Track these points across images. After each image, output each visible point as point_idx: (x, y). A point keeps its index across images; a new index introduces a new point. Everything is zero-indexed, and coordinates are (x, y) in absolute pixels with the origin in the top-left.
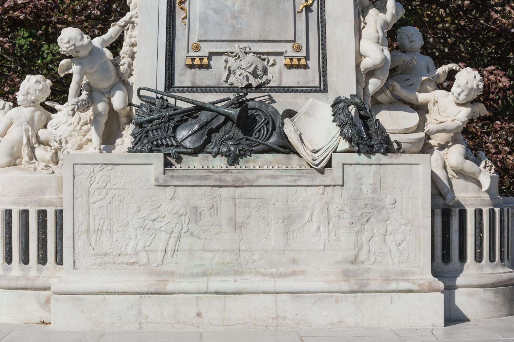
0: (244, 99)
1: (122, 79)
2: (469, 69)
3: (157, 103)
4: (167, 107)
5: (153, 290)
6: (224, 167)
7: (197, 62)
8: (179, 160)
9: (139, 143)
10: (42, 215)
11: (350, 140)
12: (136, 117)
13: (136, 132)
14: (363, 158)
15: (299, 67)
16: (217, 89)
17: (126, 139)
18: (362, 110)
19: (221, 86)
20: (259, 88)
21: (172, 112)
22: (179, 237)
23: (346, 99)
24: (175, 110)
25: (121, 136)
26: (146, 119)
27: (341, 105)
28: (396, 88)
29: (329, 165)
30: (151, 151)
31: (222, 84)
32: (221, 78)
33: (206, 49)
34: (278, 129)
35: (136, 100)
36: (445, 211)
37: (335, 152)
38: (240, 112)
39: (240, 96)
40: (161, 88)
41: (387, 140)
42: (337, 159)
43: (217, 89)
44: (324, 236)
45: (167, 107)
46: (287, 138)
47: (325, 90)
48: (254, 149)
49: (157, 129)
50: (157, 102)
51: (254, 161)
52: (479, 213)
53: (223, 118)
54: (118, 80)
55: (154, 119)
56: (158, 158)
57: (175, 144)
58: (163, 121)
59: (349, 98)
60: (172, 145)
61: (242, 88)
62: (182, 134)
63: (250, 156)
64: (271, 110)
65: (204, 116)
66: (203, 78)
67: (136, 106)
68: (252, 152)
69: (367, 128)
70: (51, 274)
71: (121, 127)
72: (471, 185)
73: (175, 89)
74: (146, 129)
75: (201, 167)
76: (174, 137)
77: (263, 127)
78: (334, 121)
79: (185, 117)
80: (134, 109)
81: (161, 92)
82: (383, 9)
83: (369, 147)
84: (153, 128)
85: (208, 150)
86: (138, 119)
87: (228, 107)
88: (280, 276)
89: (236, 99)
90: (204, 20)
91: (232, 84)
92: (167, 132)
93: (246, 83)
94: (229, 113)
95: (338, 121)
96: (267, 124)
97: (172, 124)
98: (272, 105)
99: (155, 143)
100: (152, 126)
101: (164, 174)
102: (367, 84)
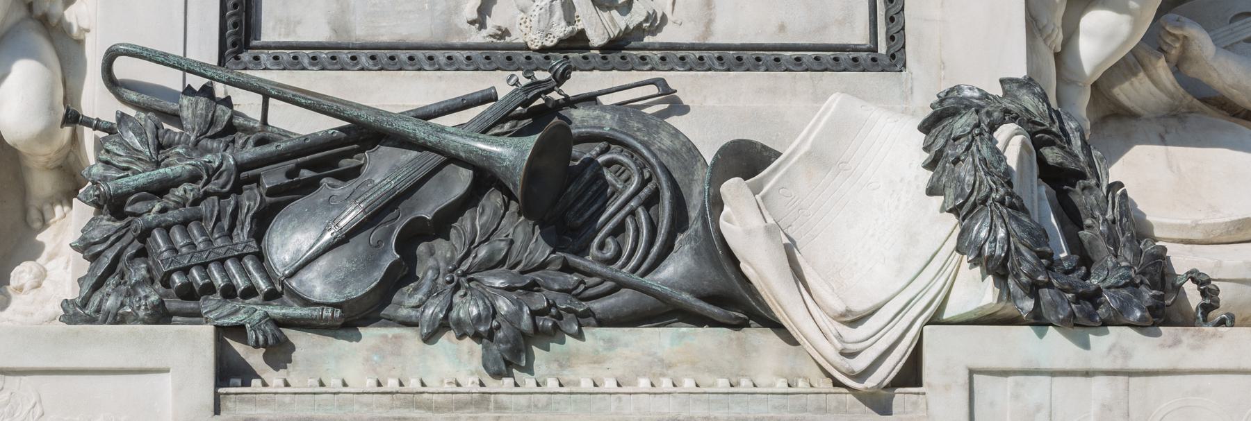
0: (554, 95)
1: (38, 12)
3: (186, 114)
4: (230, 129)
6: (469, 384)
8: (279, 354)
9: (112, 281)
11: (999, 270)
12: (98, 170)
13: (96, 235)
14: (1055, 346)
16: (441, 56)
18: (1050, 143)
19: (456, 41)
20: (618, 49)
21: (250, 153)
23: (985, 96)
24: (261, 142)
25: (34, 251)
26: (141, 179)
27: (962, 124)
28: (1195, 49)
29: (911, 374)
30: (160, 315)
31: (460, 32)
32: (457, 9)
34: (695, 225)
35: (96, 101)
37: (935, 320)
38: (538, 151)
39: (536, 84)
40: (205, 49)
41: (1157, 270)
42: (947, 353)
43: (441, 56)
45: (230, 129)
46: (735, 262)
47: (895, 61)
48: (596, 306)
49: (185, 224)
50: (189, 109)
51: (597, 360)
53: (462, 179)
54: (21, 13)
55: (175, 182)
56: (191, 346)
57: (263, 285)
58: (211, 187)
59: (997, 91)
60: (250, 292)
61: (543, 49)
62: (291, 242)
63: (579, 336)
64: (666, 141)
67: (96, 125)
68: (588, 318)
69: (1071, 217)
71: (34, 214)
73: (264, 56)
74: (140, 222)
75: (370, 384)
76: (260, 257)
77: (633, 213)
78: (931, 191)
79: (306, 174)
80: (89, 136)
81: (202, 64)
83: (1079, 298)
84: (170, 216)
85: (403, 312)
86: (105, 179)
87: (485, 129)
89: (522, 97)
91: (505, 33)
92: (229, 234)
93: (560, 30)
94: (489, 156)
95: (950, 192)
96: (652, 200)
97: (251, 201)
98: (674, 121)
99: (177, 280)
100: (164, 210)
101: (217, 411)
102: (1071, 33)
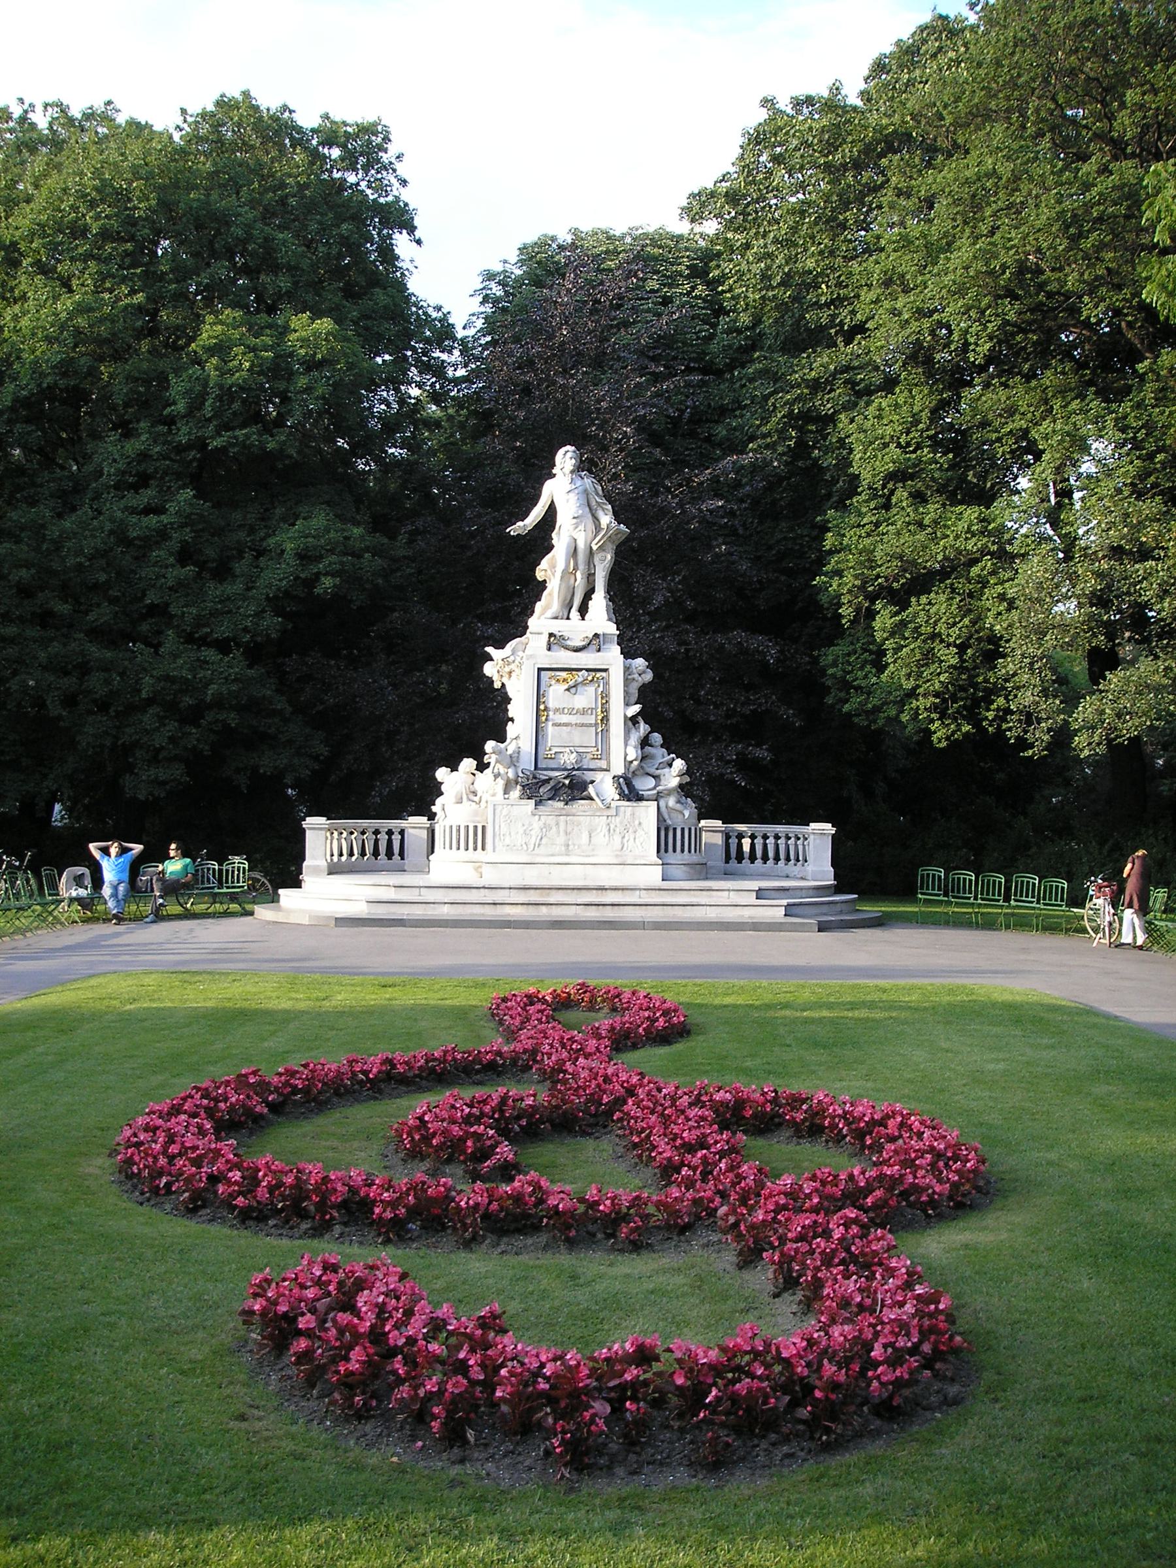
33: (554, 750)
36: (664, 829)
52: (683, 830)
65: (552, 783)
72: (680, 816)
82: (638, 729)
90: (553, 737)
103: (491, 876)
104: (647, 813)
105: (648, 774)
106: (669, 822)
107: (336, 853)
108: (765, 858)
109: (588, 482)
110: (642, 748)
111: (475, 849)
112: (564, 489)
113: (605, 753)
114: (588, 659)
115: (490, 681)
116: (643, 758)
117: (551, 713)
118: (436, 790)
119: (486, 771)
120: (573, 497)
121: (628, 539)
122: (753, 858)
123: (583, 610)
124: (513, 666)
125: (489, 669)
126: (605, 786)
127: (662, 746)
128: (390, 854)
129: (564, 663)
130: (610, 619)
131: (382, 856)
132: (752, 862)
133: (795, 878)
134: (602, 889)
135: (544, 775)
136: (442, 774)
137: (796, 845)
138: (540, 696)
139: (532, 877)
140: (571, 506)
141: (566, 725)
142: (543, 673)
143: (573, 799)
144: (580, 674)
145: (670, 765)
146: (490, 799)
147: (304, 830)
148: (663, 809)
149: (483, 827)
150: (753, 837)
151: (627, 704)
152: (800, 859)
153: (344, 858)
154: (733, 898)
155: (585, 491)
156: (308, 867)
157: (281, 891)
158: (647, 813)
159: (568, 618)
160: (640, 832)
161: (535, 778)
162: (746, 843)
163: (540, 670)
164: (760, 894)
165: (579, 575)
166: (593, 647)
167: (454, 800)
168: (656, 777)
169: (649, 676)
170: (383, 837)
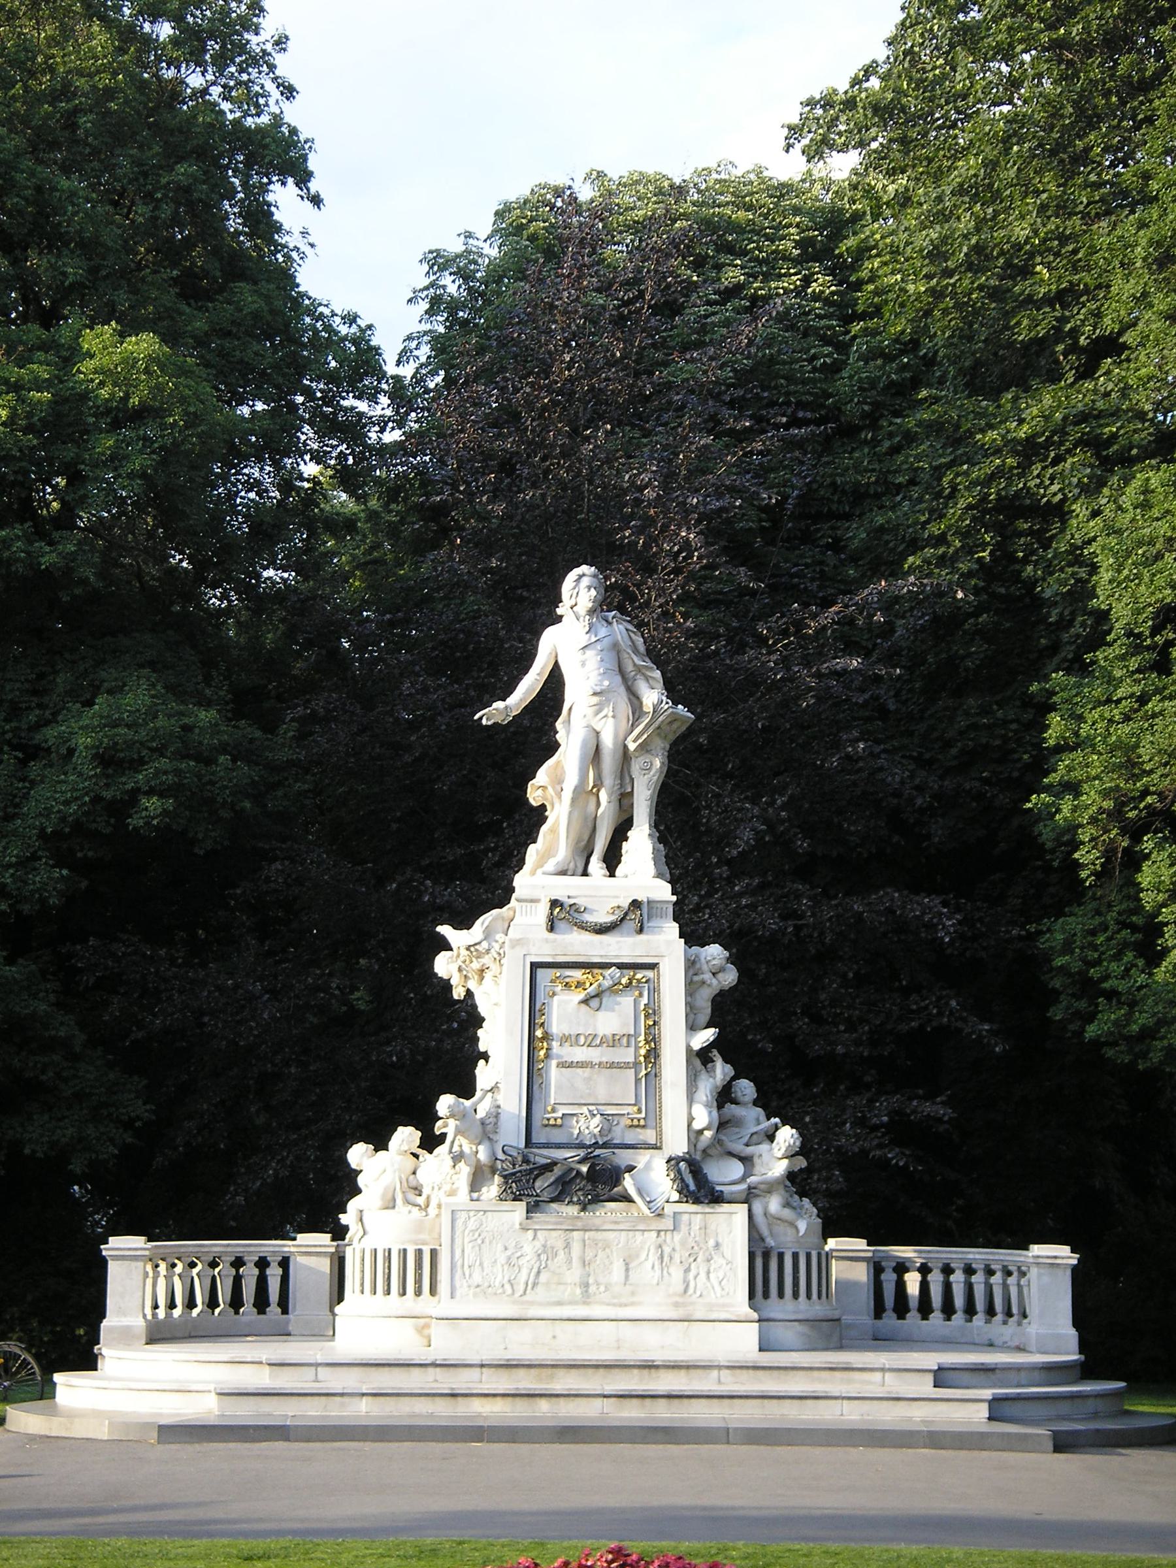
2: (788, 1127)
5: (516, 1316)
7: (552, 1122)
10: (419, 1253)
11: (680, 1192)
15: (638, 1126)
17: (492, 1189)
20: (605, 1145)
22: (539, 1272)
27: (673, 1162)
40: (522, 1144)
44: (658, 1272)
47: (660, 1148)
52: (795, 1256)
56: (521, 1207)
65: (557, 1171)
66: (557, 1136)
70: (426, 1304)
72: (791, 1231)
88: (621, 1305)
90: (558, 1087)
103: (446, 1343)
104: (731, 1226)
105: (731, 1154)
106: (770, 1242)
107: (162, 1302)
108: (948, 1310)
109: (620, 629)
110: (720, 1107)
111: (418, 1292)
112: (576, 642)
113: (653, 1116)
114: (622, 947)
115: (447, 986)
116: (723, 1125)
117: (555, 1044)
118: (346, 1184)
119: (436, 1151)
120: (592, 657)
121: (690, 732)
122: (925, 1309)
123: (612, 860)
124: (486, 960)
125: (443, 965)
126: (653, 1176)
127: (756, 1103)
128: (261, 1303)
129: (578, 957)
130: (659, 875)
131: (248, 1308)
132: (925, 1317)
133: (1005, 1348)
134: (649, 1366)
135: (542, 1156)
136: (358, 1154)
137: (1005, 1286)
138: (535, 1013)
139: (522, 1343)
140: (588, 673)
141: (582, 1065)
142: (540, 972)
143: (597, 1200)
144: (607, 972)
145: (771, 1138)
146: (445, 1200)
147: (103, 1263)
148: (760, 1219)
149: (434, 1253)
150: (924, 1270)
151: (692, 1027)
152: (1015, 1312)
153: (177, 1312)
154: (889, 1385)
155: (615, 647)
156: (111, 1329)
157: (58, 1377)
158: (731, 1226)
159: (585, 873)
160: (718, 1261)
161: (526, 1161)
162: (913, 1282)
163: (535, 966)
164: (942, 1376)
165: (604, 796)
166: (631, 925)
167: (379, 1203)
168: (746, 1160)
169: (730, 977)
170: (250, 1273)
